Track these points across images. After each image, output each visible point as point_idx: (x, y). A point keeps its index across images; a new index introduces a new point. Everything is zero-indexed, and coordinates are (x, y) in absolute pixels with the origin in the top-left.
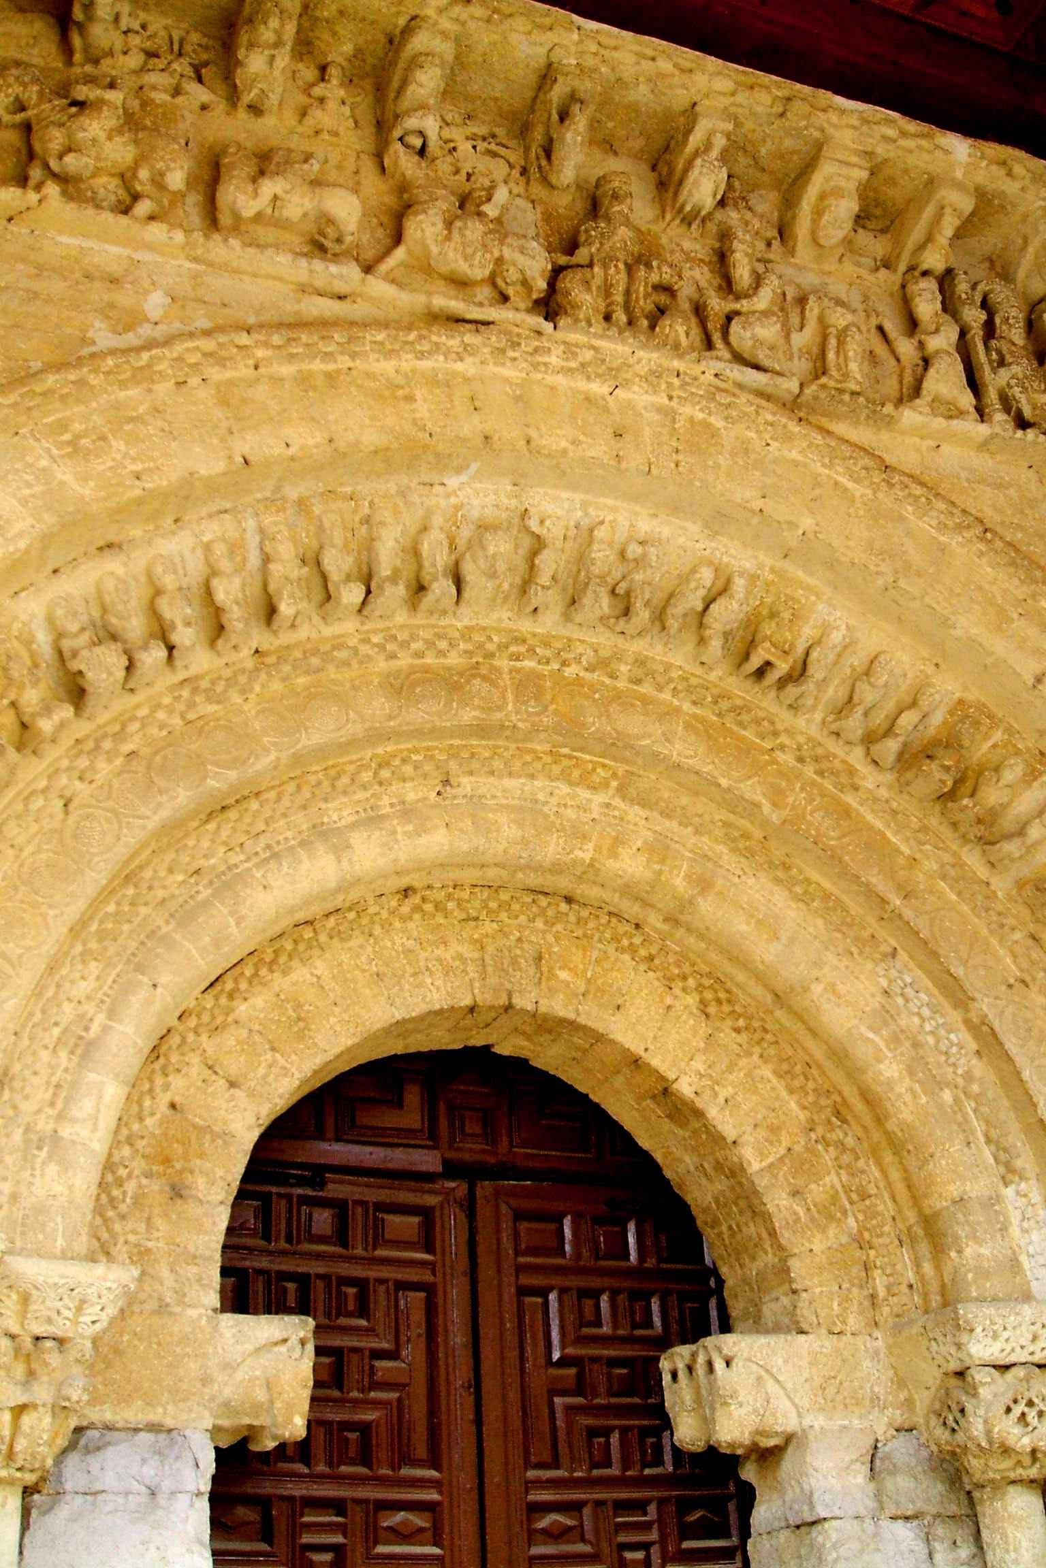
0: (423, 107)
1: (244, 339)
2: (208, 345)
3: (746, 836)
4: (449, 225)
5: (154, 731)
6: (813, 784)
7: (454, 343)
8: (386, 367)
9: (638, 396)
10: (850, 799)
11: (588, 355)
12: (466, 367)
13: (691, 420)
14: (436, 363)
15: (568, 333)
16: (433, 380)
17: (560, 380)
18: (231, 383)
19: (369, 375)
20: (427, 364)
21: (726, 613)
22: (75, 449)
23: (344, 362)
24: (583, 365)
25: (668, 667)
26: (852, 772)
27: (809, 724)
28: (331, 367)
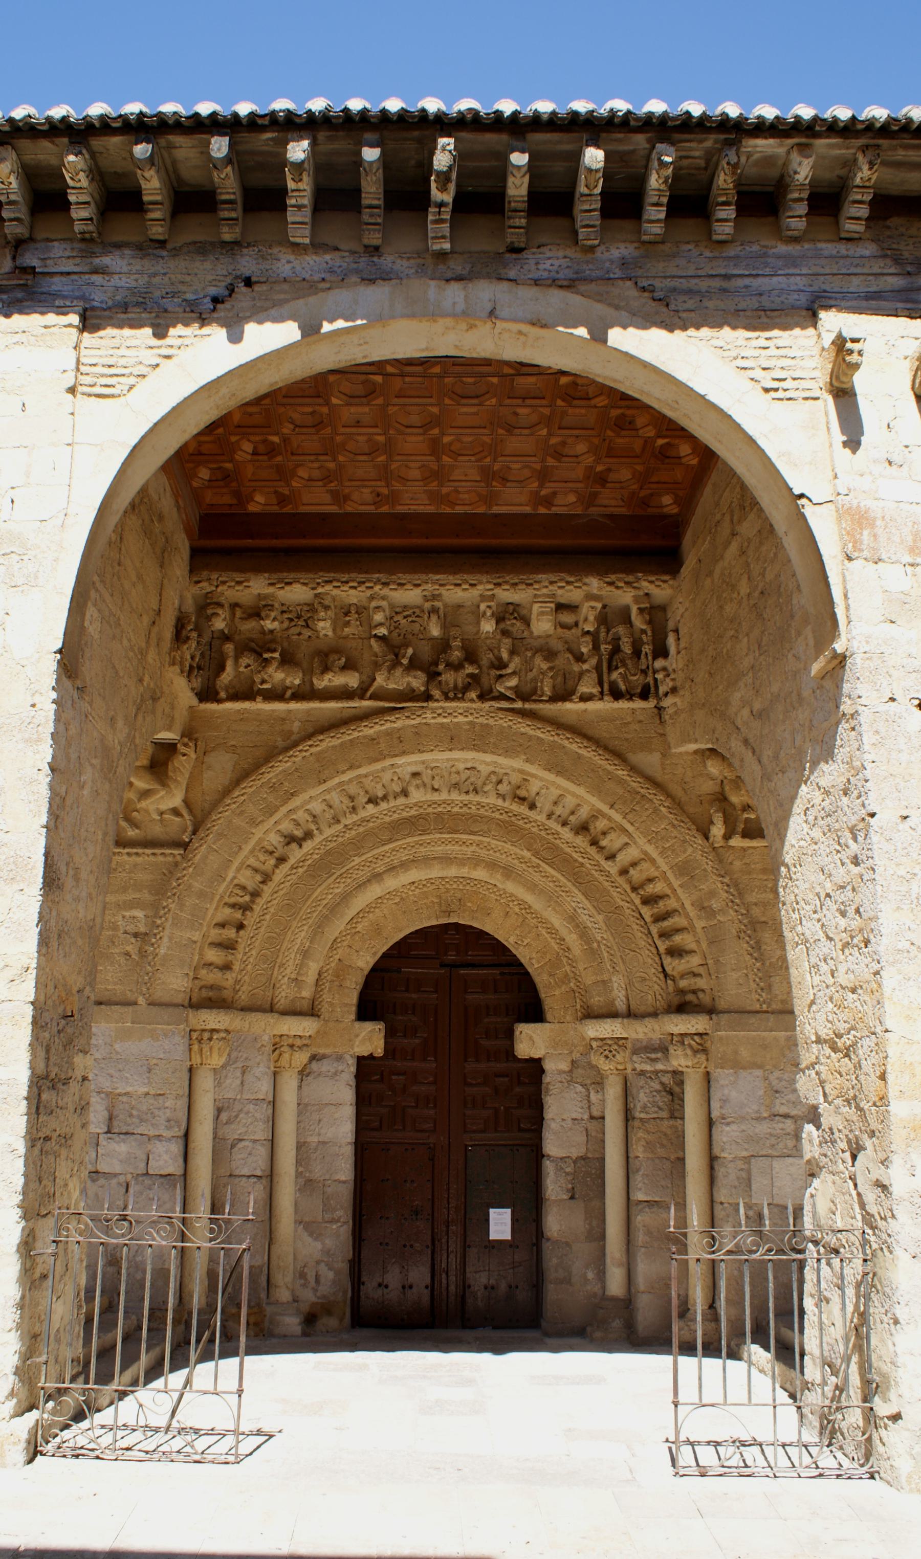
0: (381, 624)
1: (321, 737)
2: (310, 743)
3: (523, 858)
4: (389, 672)
5: (316, 856)
6: (545, 839)
7: (393, 718)
8: (371, 731)
9: (461, 719)
10: (558, 841)
11: (440, 711)
12: (399, 724)
13: (482, 725)
14: (388, 725)
15: (432, 704)
16: (389, 734)
17: (433, 721)
18: (320, 753)
19: (365, 737)
20: (383, 728)
21: (504, 788)
22: (273, 788)
23: (356, 734)
24: (439, 715)
25: (488, 804)
26: (558, 833)
27: (542, 818)
28: (351, 737)
